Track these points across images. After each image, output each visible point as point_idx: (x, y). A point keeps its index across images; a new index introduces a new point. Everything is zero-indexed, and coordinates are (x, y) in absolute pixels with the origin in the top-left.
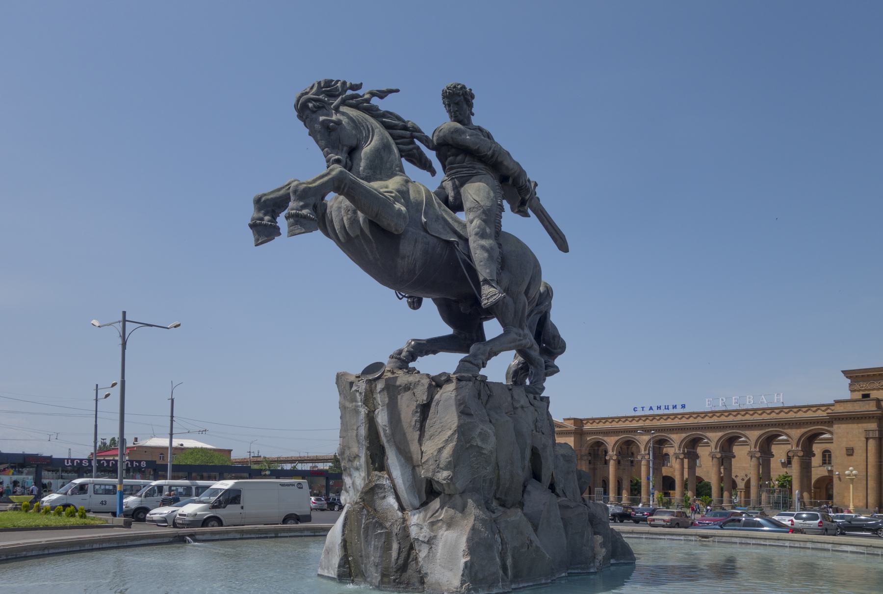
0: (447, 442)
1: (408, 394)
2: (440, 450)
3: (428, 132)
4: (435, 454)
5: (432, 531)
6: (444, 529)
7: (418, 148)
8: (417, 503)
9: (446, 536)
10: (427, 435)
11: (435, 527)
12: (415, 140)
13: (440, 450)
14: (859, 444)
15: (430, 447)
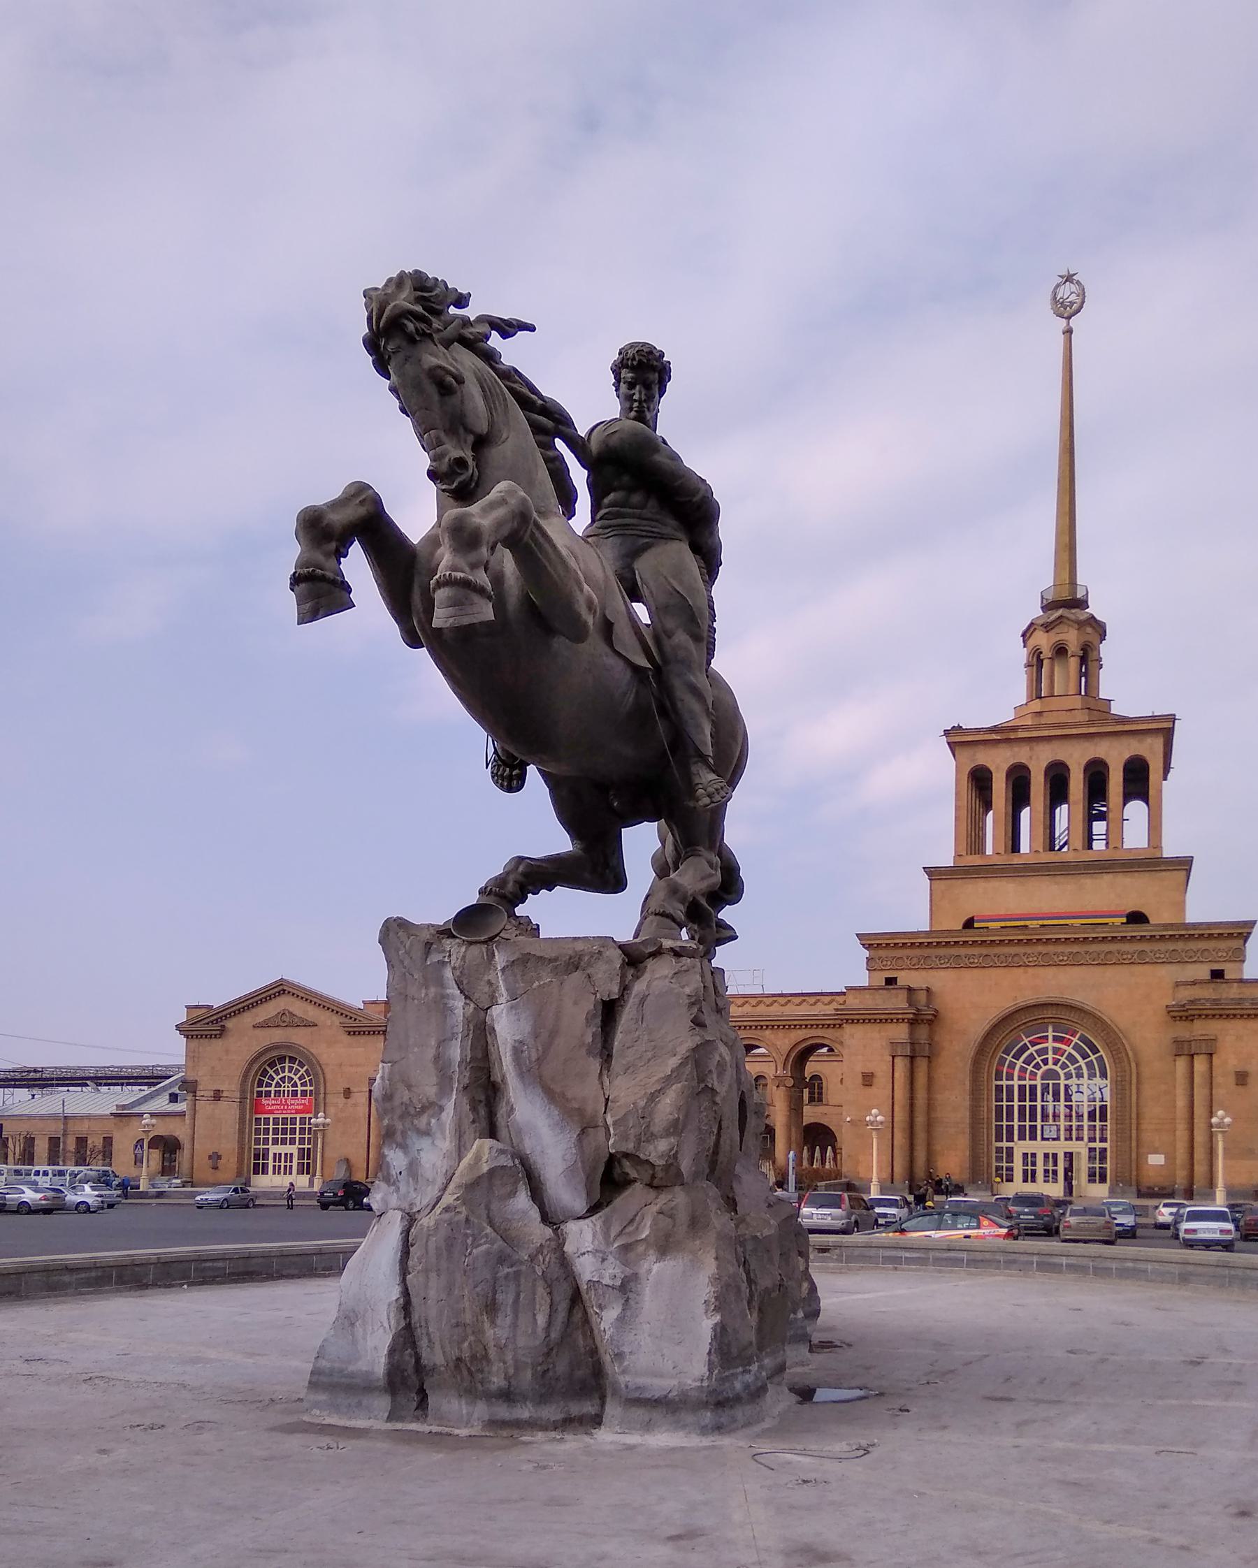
0: (668, 1081)
1: (577, 976)
2: (653, 1097)
3: (582, 432)
4: (642, 1103)
5: (626, 1263)
6: (653, 1258)
7: (560, 458)
8: (580, 1205)
9: (655, 1270)
10: (616, 1064)
11: (632, 1255)
12: (559, 443)
13: (653, 1097)
14: (881, 1067)
15: (626, 1090)
